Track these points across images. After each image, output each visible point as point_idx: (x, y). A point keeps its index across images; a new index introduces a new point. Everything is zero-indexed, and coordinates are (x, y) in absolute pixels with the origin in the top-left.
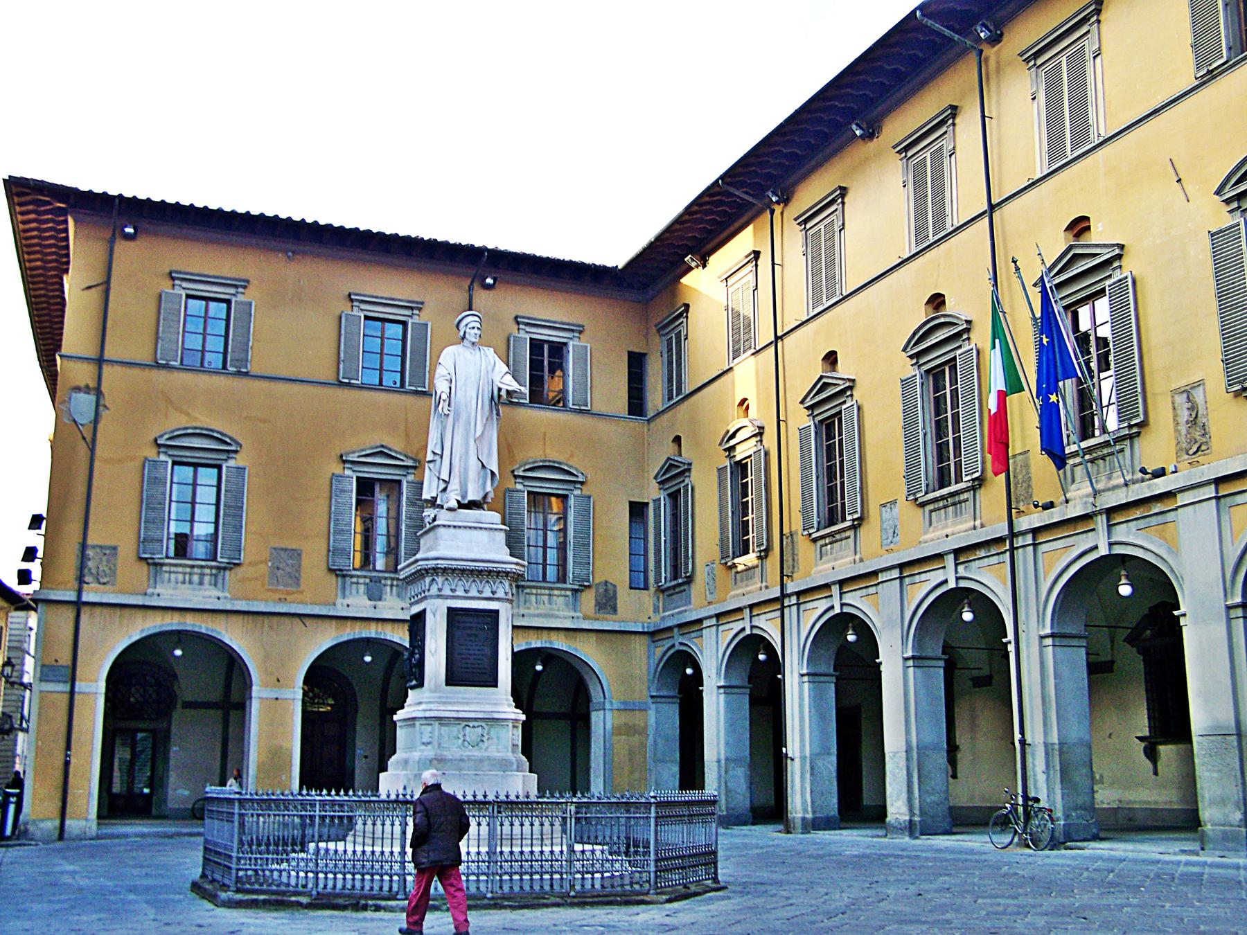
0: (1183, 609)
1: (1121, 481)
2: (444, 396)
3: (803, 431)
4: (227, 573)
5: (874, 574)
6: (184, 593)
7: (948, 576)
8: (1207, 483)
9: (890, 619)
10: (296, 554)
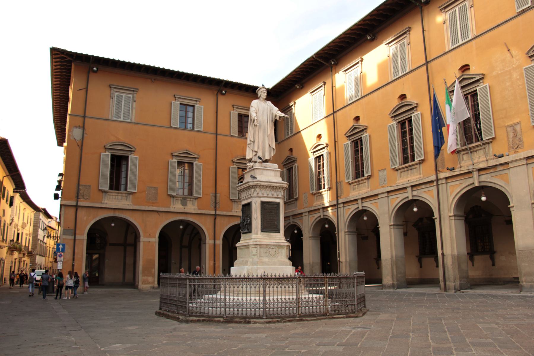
0: (511, 205)
1: (485, 159)
2: (256, 118)
3: (346, 146)
4: (131, 196)
5: (377, 195)
6: (116, 202)
7: (409, 195)
8: (523, 159)
9: (384, 212)
10: (156, 189)
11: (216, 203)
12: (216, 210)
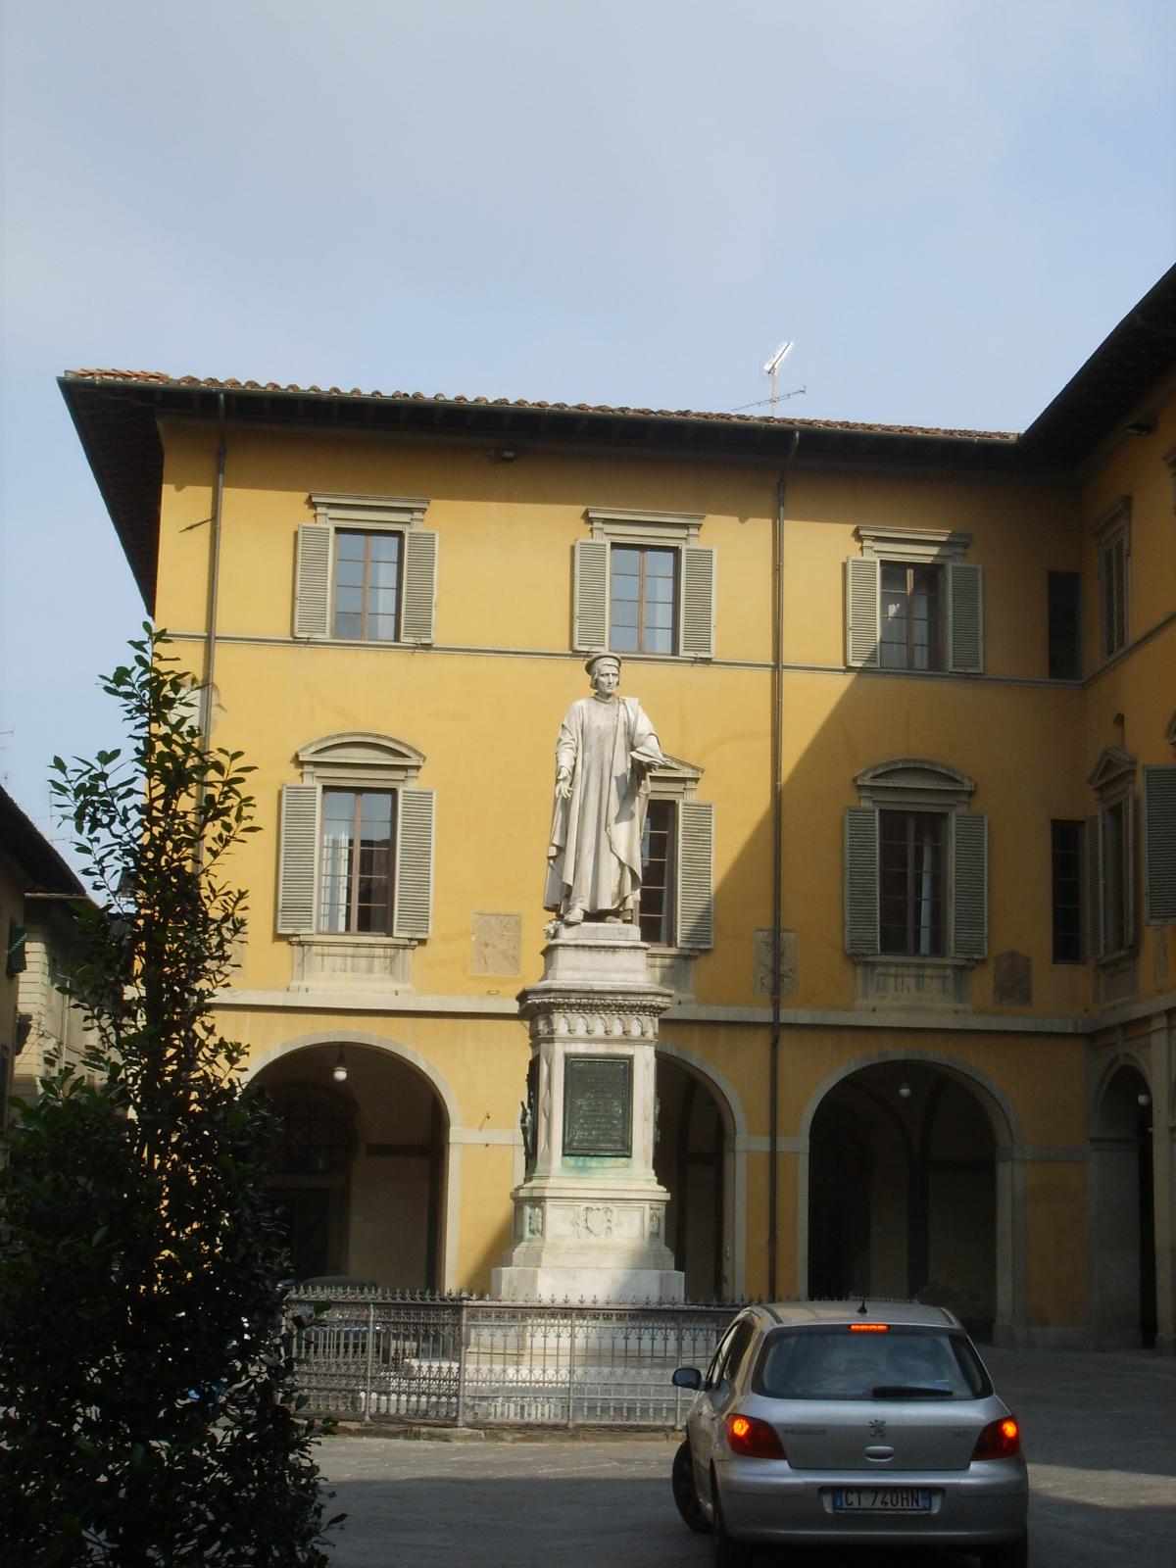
11: (777, 974)
12: (776, 1005)
